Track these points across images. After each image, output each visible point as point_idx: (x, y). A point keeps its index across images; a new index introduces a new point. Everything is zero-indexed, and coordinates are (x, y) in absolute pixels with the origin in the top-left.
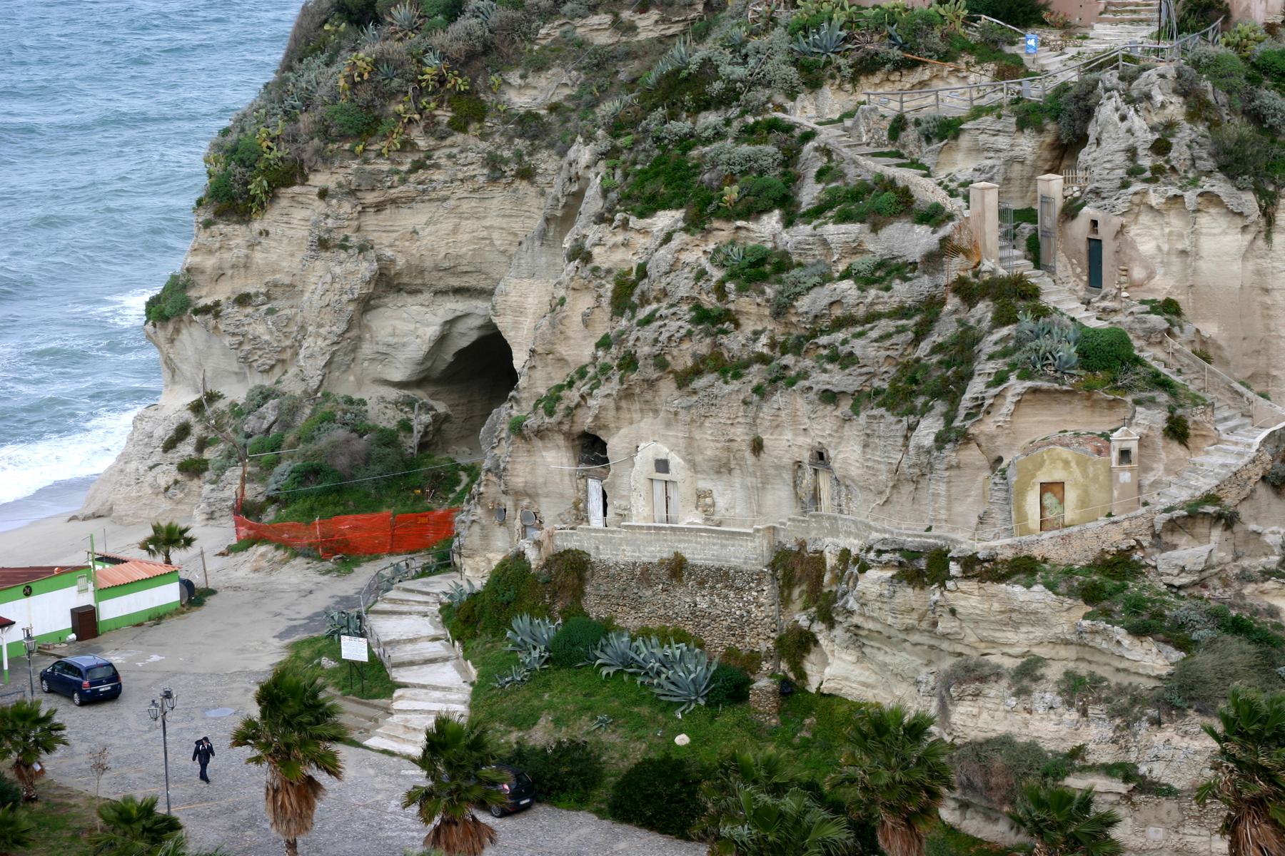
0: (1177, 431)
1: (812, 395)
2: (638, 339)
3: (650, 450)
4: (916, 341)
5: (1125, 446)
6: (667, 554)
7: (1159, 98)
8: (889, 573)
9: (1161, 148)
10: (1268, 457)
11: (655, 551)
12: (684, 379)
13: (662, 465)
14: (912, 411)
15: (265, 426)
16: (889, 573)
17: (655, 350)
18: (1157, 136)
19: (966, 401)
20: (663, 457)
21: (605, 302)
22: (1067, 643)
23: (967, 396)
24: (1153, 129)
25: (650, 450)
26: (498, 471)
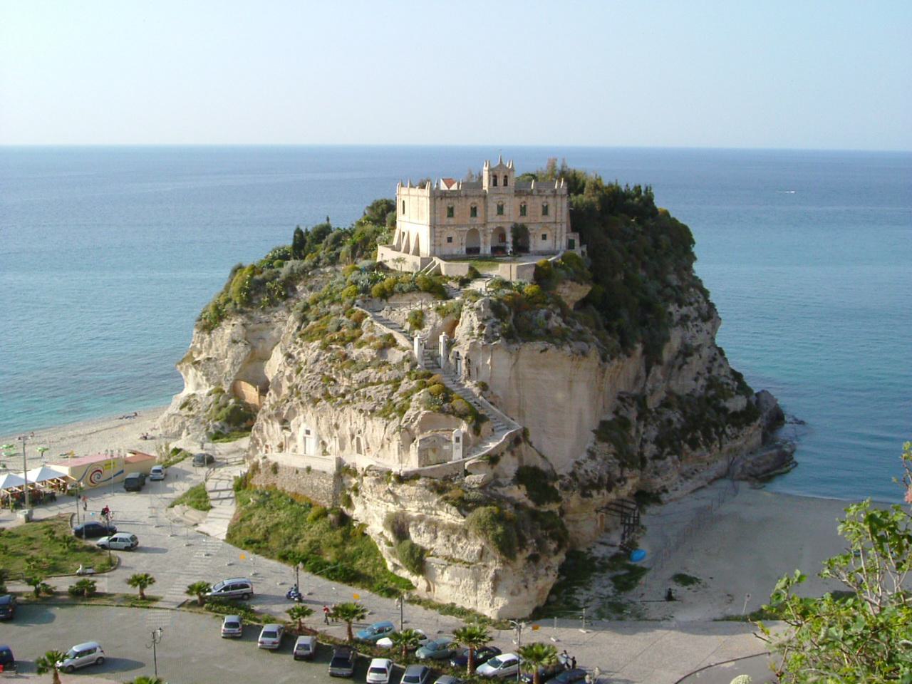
0: (476, 430)
1: (356, 410)
2: (301, 387)
3: (304, 427)
4: (392, 393)
5: (458, 436)
6: (305, 467)
7: (482, 309)
8: (374, 478)
9: (481, 327)
10: (508, 442)
11: (300, 463)
12: (315, 401)
13: (308, 432)
14: (388, 419)
15: (209, 403)
16: (374, 478)
17: (307, 391)
18: (480, 323)
19: (405, 417)
20: (308, 429)
21: (294, 371)
22: (432, 509)
23: (407, 413)
24: (479, 320)
25: (304, 427)
26: (260, 430)
